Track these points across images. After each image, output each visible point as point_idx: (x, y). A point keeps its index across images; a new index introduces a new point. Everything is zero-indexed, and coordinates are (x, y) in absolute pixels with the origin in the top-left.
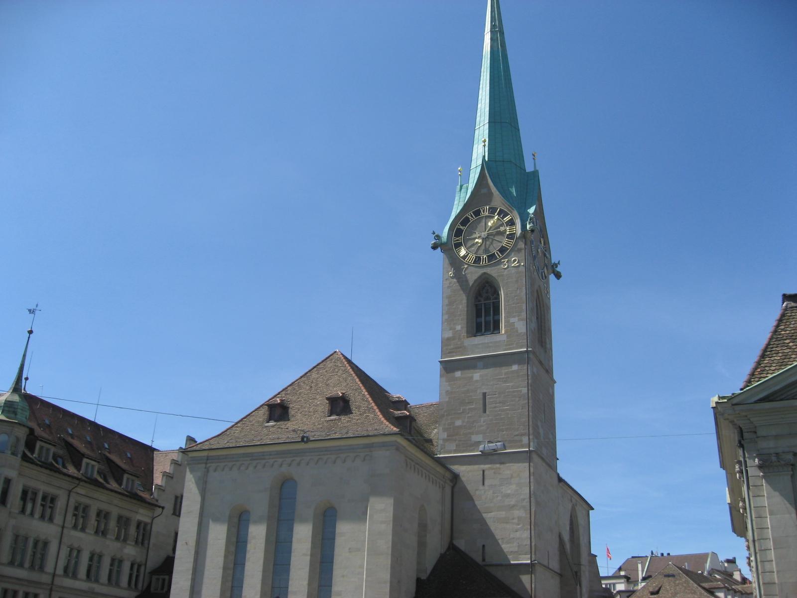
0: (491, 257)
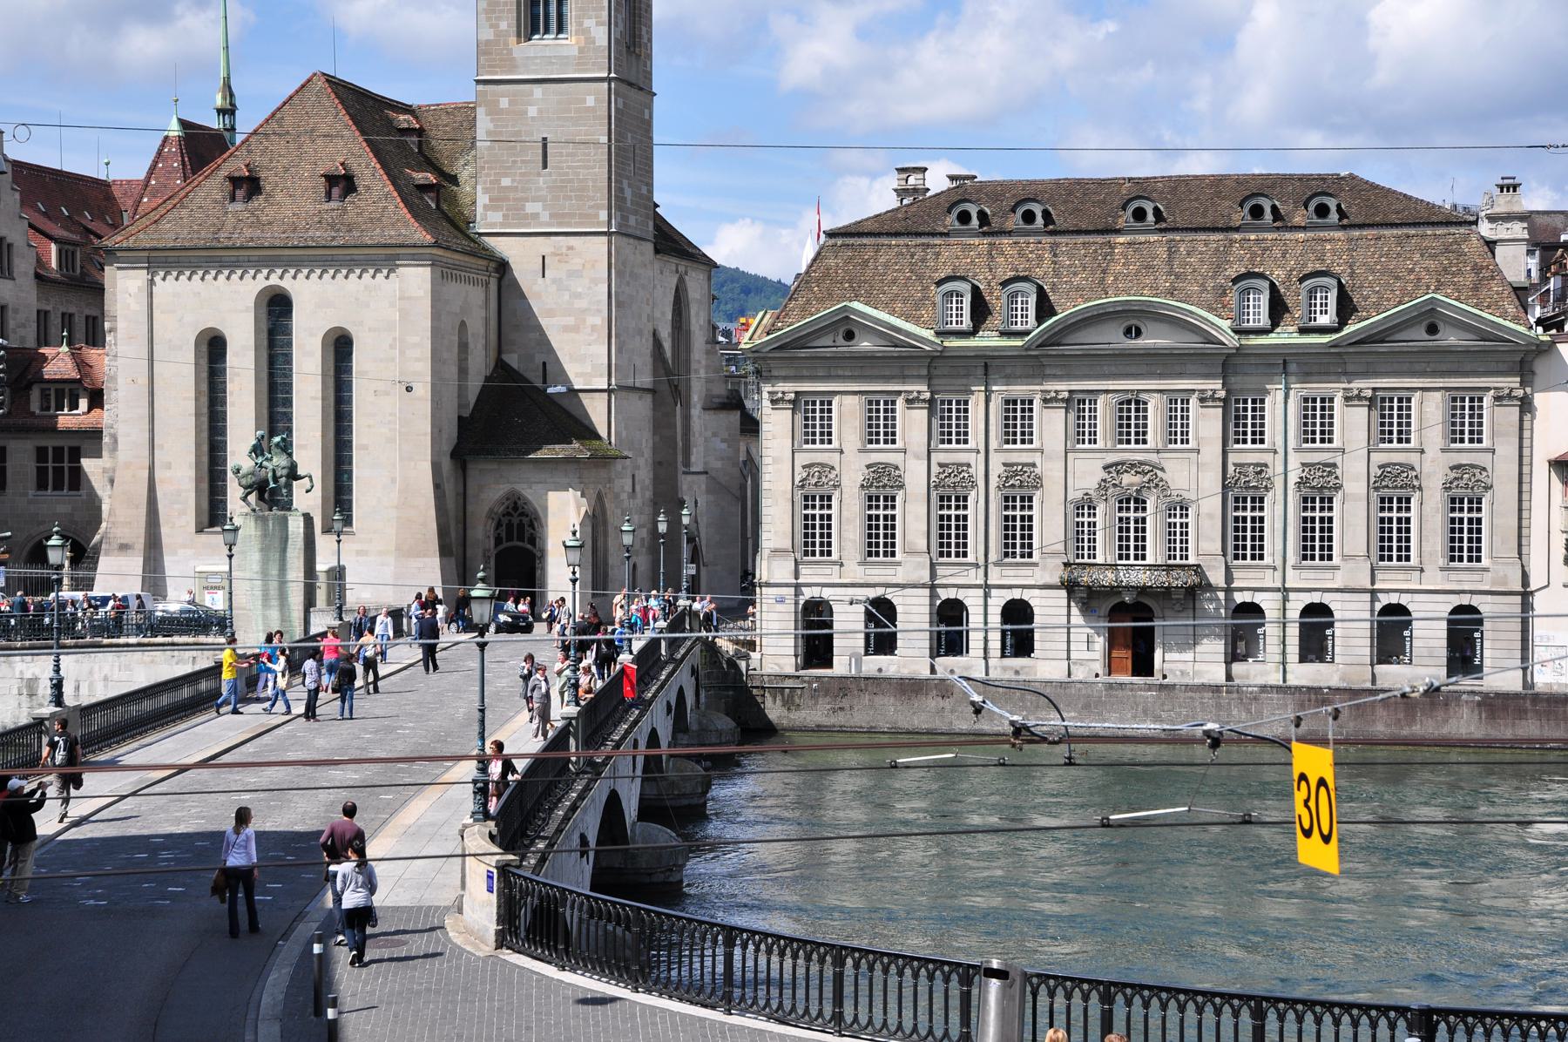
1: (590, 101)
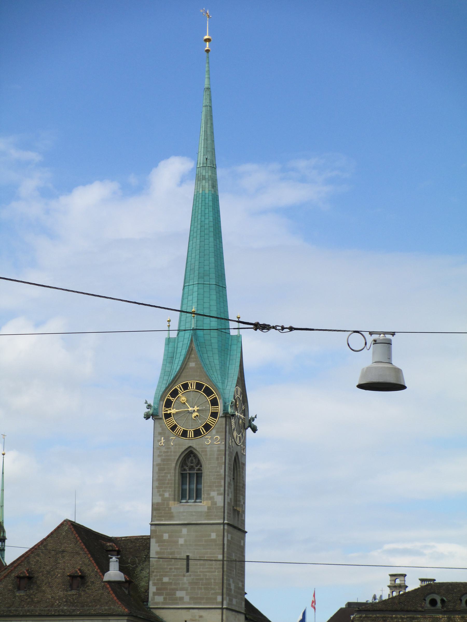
0: (197, 433)
1: (213, 536)
